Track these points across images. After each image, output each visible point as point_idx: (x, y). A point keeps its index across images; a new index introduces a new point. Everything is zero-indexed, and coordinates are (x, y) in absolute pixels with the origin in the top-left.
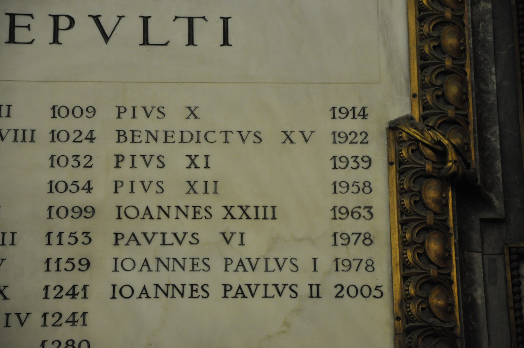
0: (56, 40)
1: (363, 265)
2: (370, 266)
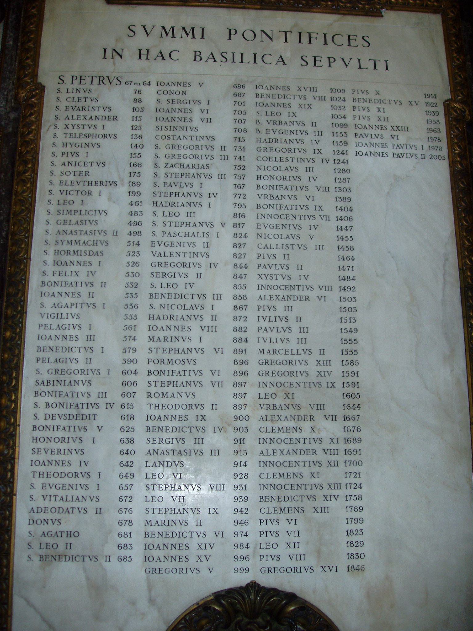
0: (330, 66)
1: (438, 148)
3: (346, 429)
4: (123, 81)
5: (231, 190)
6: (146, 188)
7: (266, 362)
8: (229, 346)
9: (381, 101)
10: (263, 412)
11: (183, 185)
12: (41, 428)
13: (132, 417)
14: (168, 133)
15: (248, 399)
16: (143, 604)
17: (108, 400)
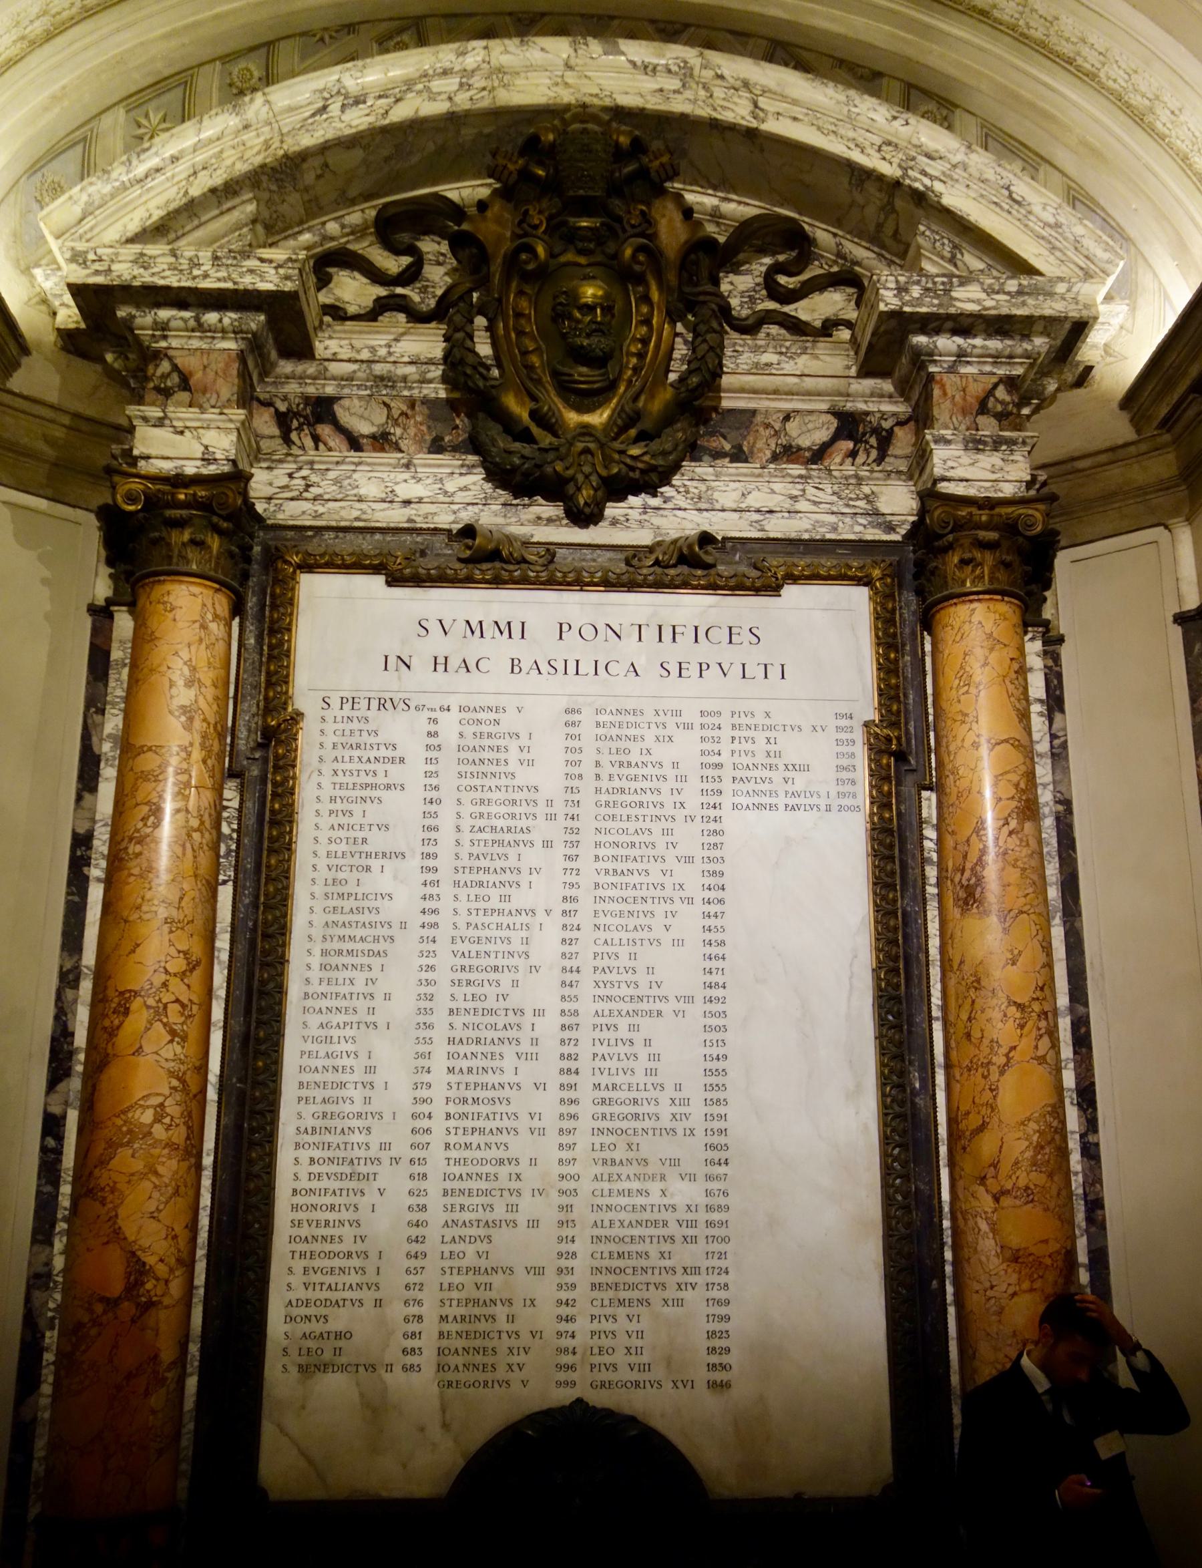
2: (854, 796)
3: (708, 1193)
4: (412, 706)
5: (561, 863)
6: (445, 863)
7: (603, 1102)
8: (554, 1080)
9: (771, 728)
10: (598, 1170)
11: (495, 857)
12: (303, 1192)
13: (425, 1175)
14: (477, 782)
15: (578, 1152)
16: (435, 1431)
17: (394, 1153)
